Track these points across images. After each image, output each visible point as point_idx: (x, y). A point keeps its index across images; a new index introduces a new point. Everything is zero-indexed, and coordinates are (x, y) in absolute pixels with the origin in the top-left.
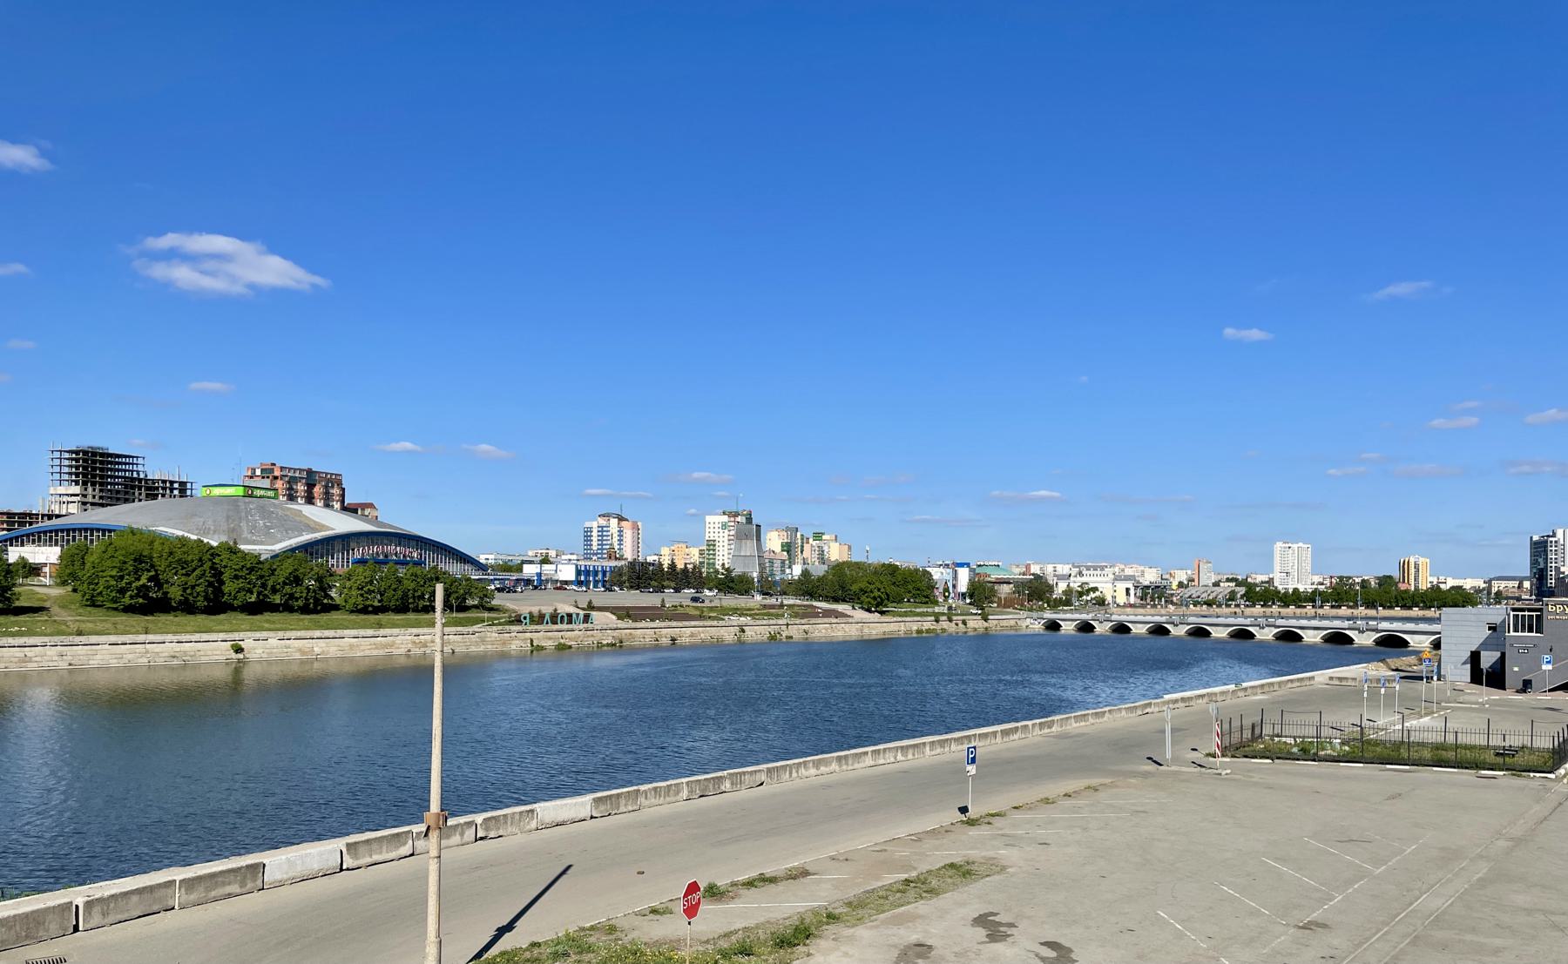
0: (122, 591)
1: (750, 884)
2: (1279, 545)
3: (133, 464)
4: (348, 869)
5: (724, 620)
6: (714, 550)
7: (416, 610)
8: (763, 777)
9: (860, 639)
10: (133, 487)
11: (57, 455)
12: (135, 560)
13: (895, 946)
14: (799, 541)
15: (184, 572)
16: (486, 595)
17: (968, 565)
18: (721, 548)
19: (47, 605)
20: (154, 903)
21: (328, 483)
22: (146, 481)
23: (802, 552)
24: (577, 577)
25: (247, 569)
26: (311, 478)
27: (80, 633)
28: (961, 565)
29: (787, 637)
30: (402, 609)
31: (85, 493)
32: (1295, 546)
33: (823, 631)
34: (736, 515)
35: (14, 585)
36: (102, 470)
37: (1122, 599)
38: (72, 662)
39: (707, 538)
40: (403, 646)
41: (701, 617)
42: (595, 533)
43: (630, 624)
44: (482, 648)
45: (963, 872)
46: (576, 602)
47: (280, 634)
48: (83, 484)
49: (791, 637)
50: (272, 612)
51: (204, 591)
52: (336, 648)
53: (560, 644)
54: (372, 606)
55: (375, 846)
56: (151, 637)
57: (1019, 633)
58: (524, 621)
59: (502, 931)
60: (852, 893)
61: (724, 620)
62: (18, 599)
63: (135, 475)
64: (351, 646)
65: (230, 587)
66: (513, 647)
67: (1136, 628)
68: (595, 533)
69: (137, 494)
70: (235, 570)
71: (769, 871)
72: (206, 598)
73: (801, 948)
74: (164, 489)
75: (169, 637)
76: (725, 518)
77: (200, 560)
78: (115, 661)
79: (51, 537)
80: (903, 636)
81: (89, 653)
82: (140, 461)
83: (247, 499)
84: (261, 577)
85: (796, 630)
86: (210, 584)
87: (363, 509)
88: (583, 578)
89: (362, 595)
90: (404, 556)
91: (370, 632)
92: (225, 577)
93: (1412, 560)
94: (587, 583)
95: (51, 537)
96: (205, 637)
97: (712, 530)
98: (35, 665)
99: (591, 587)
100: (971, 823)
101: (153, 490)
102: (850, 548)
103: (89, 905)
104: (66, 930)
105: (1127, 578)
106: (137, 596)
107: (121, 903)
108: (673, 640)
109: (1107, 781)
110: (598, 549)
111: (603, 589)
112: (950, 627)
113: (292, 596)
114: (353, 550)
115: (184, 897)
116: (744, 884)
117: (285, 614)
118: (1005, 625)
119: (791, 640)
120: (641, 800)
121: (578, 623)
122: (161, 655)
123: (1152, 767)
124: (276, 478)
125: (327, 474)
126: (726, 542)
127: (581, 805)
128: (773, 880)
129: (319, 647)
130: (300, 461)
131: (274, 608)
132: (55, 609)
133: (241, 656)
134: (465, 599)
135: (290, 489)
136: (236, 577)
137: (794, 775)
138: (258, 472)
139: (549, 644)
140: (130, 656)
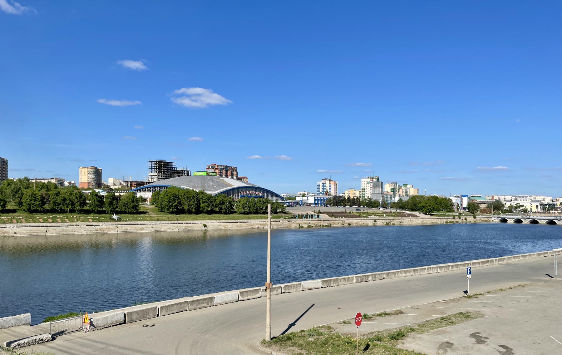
0: (170, 207)
1: (380, 315)
3: (173, 165)
4: (240, 301)
5: (368, 217)
6: (365, 191)
7: (261, 213)
8: (384, 276)
9: (422, 225)
10: (173, 173)
11: (150, 163)
12: (174, 197)
13: (438, 343)
14: (398, 188)
15: (188, 200)
16: (284, 208)
17: (467, 196)
18: (367, 191)
19: (148, 211)
20: (181, 308)
21: (232, 170)
22: (177, 171)
23: (399, 192)
24: (315, 202)
25: (208, 199)
26: (227, 169)
27: (158, 220)
28: (464, 196)
29: (393, 224)
30: (256, 213)
31: (159, 175)
33: (407, 222)
34: (373, 178)
35: (139, 205)
36: (164, 167)
37: (534, 210)
38: (156, 230)
39: (362, 187)
40: (256, 225)
41: (360, 216)
42: (321, 186)
43: (334, 218)
44: (282, 227)
45: (466, 316)
46: (314, 210)
47: (218, 221)
48: (158, 172)
49: (395, 224)
50: (215, 214)
51: (195, 207)
52: (235, 226)
53: (309, 225)
54: (246, 212)
55: (249, 293)
56: (179, 222)
57: (489, 223)
58: (297, 217)
59: (291, 325)
60: (420, 321)
61: (368, 217)
62: (140, 209)
63: (173, 169)
65: (202, 205)
66: (293, 226)
67: (541, 222)
68: (321, 186)
69: (174, 175)
70: (204, 200)
71: (387, 311)
72: (195, 209)
73: (400, 340)
74: (182, 173)
75: (184, 222)
76: (369, 180)
77: (193, 196)
78: (168, 229)
79: (149, 189)
80: (440, 224)
81: (161, 226)
82: (175, 164)
83: (207, 176)
84: (212, 202)
85: (397, 221)
86: (196, 204)
87: (243, 179)
88: (317, 202)
89: (243, 208)
90: (257, 195)
91: (246, 221)
92: (201, 202)
94: (318, 204)
95: (149, 189)
96: (195, 222)
97: (364, 184)
98: (145, 230)
99: (320, 205)
100: (469, 297)
101: (179, 173)
102: (418, 190)
103: (162, 308)
104: (155, 316)
106: (175, 208)
107: (171, 308)
108: (349, 224)
109: (528, 283)
110: (322, 192)
111: (324, 206)
112: (460, 221)
113: (221, 208)
114: (240, 193)
115: (190, 307)
116: (378, 315)
117: (219, 214)
118: (483, 220)
119: (394, 225)
120: (339, 282)
121: (315, 218)
122: (182, 227)
123: (548, 278)
125: (232, 167)
126: (369, 188)
127: (317, 283)
128: (389, 314)
129: (230, 225)
131: (216, 212)
132: (151, 212)
133: (206, 228)
134: (277, 209)
135: (221, 172)
136: (204, 202)
137: (397, 275)
138: (211, 167)
139: (305, 225)
140: (173, 228)
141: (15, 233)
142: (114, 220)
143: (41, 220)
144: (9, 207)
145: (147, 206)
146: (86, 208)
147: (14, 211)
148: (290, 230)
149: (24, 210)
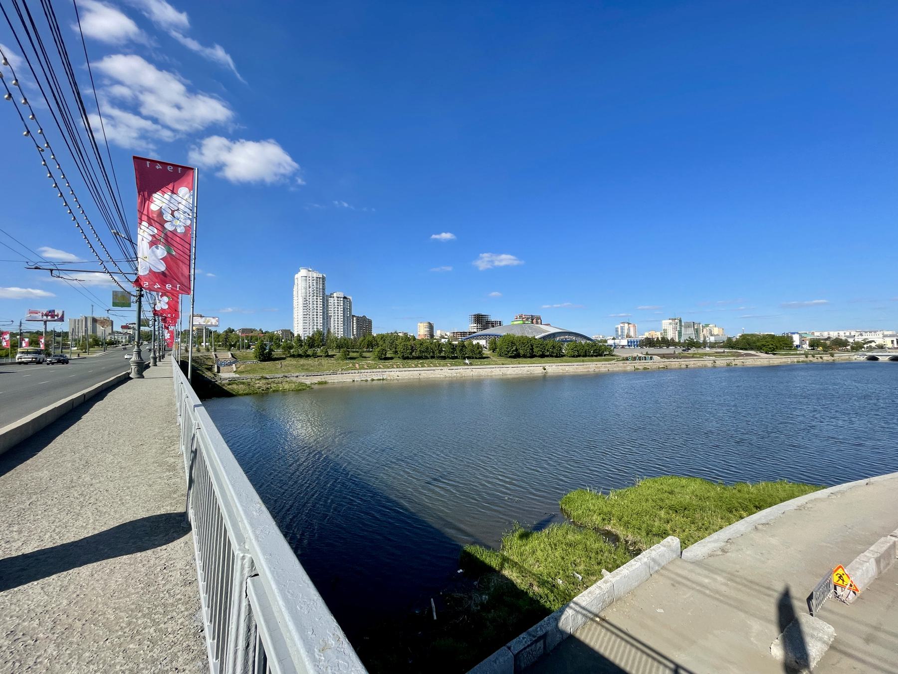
0: (508, 352)
7: (589, 356)
19: (489, 356)
23: (703, 332)
26: (532, 318)
27: (503, 364)
28: (794, 333)
29: (735, 365)
30: (585, 356)
37: (890, 345)
41: (693, 357)
42: (619, 329)
43: (666, 360)
44: (618, 369)
47: (556, 364)
56: (522, 365)
57: (852, 361)
64: (577, 368)
65: (535, 350)
68: (619, 329)
72: (530, 354)
75: (526, 365)
76: (671, 321)
80: (796, 363)
85: (739, 362)
86: (531, 349)
88: (630, 344)
91: (582, 363)
96: (533, 365)
101: (493, 324)
102: (723, 329)
105: (891, 336)
106: (512, 353)
108: (687, 366)
112: (814, 360)
113: (552, 352)
129: (567, 368)
130: (530, 313)
131: (547, 356)
132: (492, 357)
133: (545, 371)
141: (398, 376)
142: (466, 364)
143: (413, 365)
144: (388, 355)
145: (486, 352)
146: (443, 354)
147: (392, 358)
148: (625, 373)
149: (399, 357)
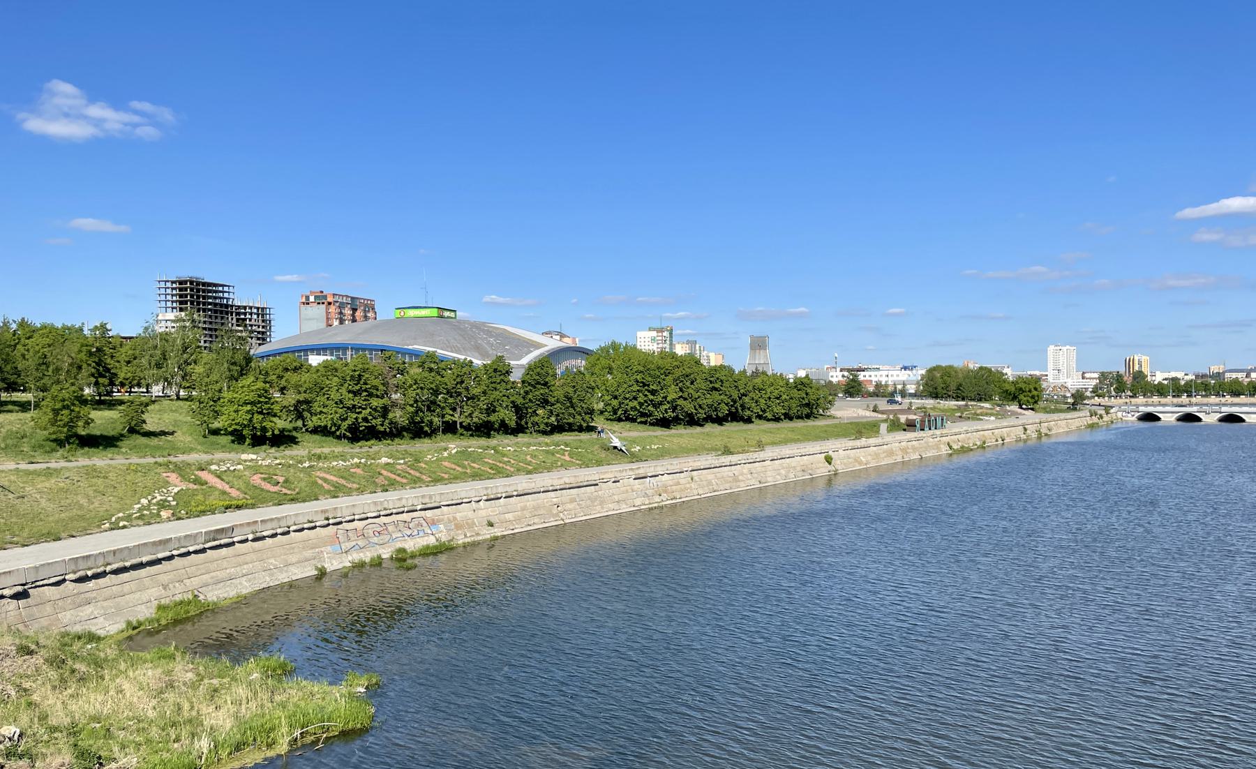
2: (1051, 348)
32: (1064, 349)
36: (204, 297)
76: (654, 334)
93: (1136, 358)
124: (330, 303)
125: (364, 300)
